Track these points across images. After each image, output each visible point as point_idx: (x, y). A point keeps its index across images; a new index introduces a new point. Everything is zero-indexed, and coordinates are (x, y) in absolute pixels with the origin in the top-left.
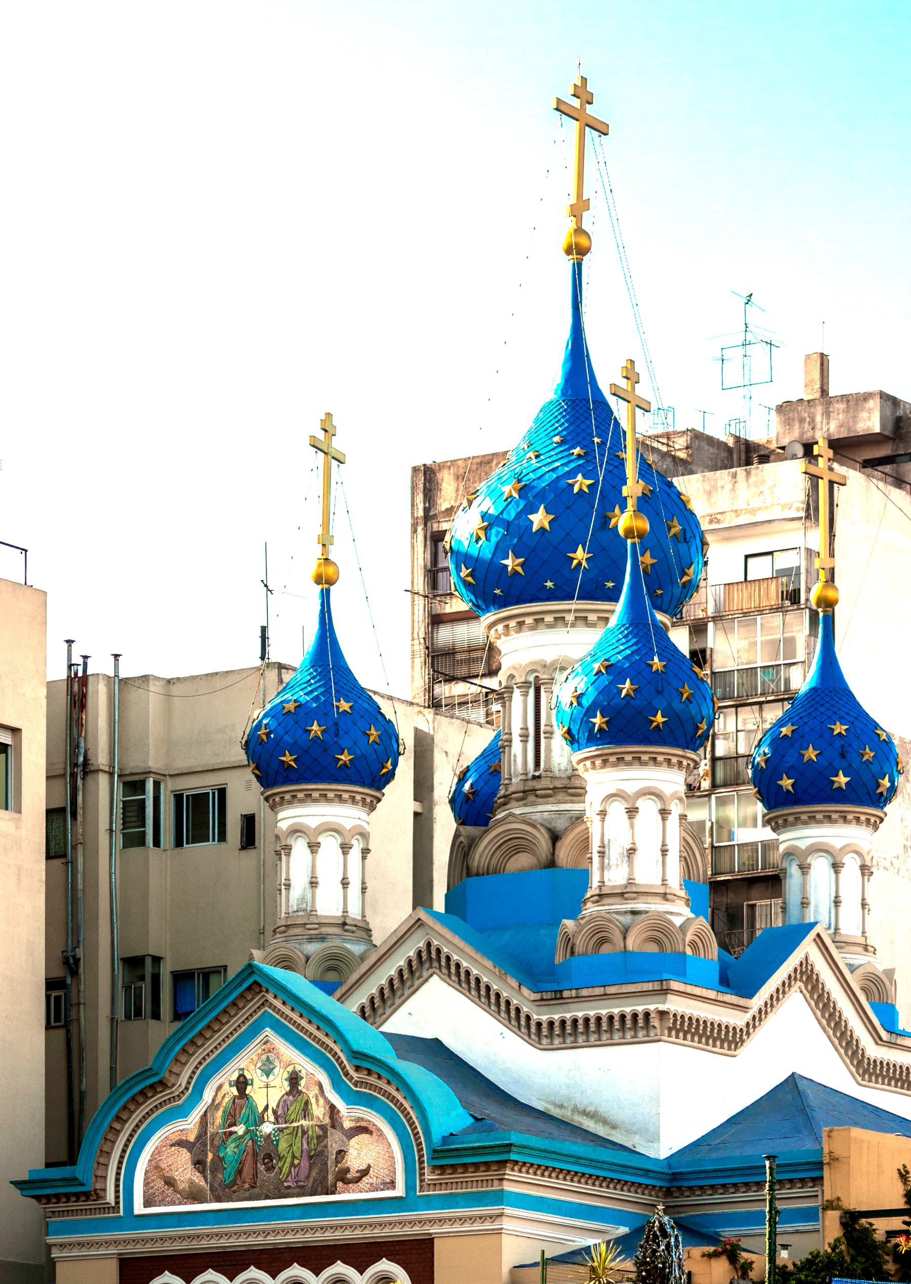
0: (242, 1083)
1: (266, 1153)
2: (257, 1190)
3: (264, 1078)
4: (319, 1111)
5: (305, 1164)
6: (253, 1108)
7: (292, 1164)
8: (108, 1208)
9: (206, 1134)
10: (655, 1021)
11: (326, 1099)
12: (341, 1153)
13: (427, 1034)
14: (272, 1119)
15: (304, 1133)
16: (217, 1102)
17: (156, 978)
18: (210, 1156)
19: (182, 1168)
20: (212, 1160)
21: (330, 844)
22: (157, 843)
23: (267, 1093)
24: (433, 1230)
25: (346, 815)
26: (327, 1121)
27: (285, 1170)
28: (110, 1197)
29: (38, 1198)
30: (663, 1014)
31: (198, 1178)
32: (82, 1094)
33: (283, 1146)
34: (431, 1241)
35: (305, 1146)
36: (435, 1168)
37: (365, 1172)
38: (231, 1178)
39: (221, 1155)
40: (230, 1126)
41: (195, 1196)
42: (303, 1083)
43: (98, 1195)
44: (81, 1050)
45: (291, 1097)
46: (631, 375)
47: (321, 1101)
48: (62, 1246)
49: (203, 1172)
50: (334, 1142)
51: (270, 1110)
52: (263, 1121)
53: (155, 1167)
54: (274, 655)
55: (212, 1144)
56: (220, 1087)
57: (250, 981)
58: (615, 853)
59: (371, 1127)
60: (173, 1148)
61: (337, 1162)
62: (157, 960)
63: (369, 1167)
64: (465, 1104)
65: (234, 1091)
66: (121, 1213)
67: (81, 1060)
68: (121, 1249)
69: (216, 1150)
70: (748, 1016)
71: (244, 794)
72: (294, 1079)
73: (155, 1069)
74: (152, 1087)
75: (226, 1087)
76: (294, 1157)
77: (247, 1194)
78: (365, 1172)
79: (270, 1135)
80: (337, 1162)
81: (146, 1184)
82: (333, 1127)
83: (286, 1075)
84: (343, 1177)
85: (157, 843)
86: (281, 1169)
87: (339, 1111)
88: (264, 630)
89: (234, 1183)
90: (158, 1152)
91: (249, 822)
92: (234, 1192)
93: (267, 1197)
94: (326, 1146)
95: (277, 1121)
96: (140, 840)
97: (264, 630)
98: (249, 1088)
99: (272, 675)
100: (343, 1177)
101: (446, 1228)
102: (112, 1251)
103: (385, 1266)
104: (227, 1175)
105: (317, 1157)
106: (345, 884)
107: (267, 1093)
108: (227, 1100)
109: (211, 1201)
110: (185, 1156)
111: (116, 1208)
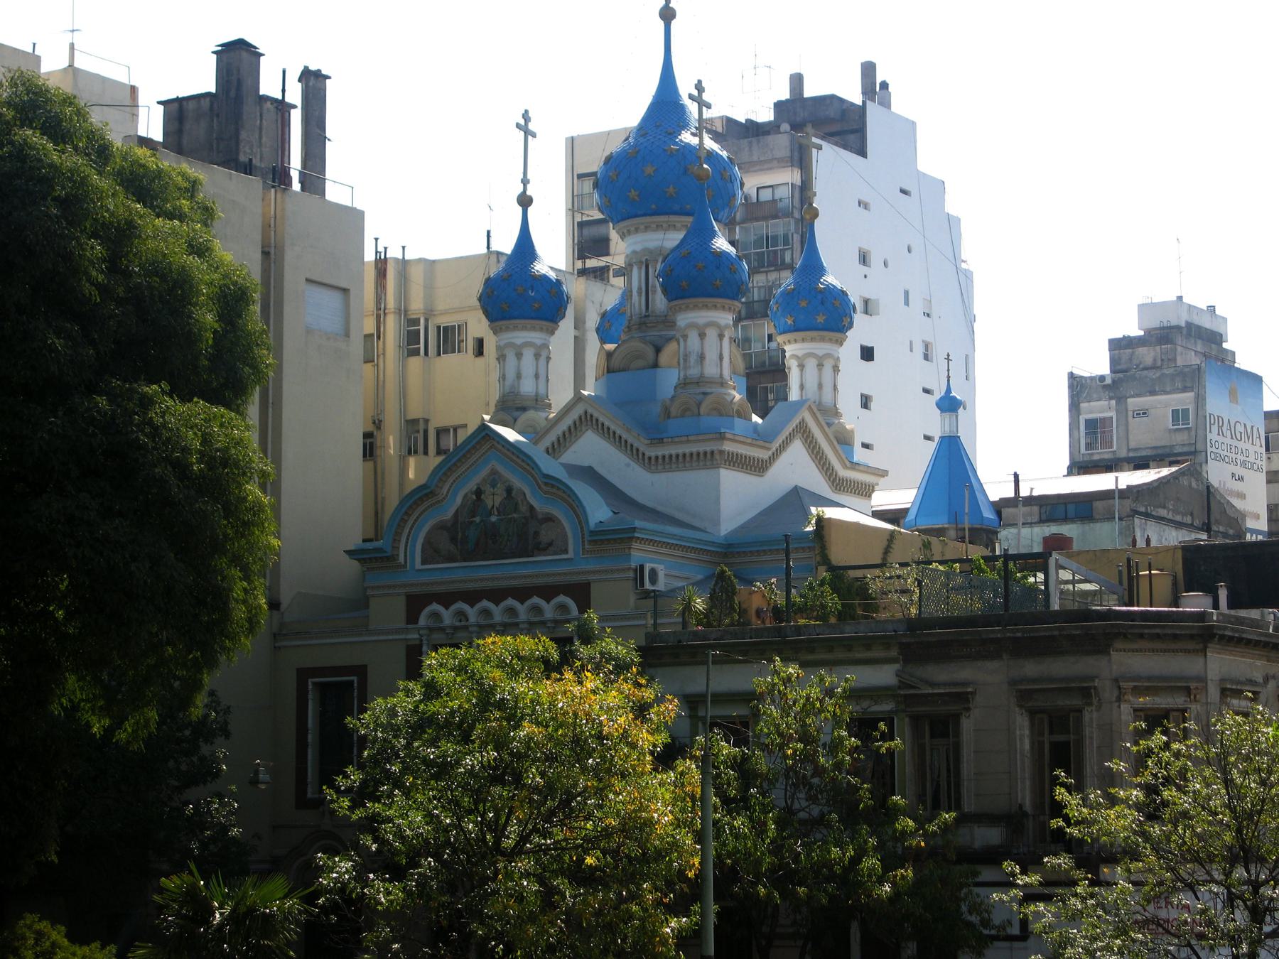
8: (400, 566)
10: (717, 456)
12: (536, 533)
13: (586, 464)
17: (426, 432)
21: (528, 355)
22: (426, 353)
23: (493, 499)
25: (536, 337)
26: (528, 514)
29: (359, 560)
30: (721, 452)
32: (383, 498)
36: (590, 542)
37: (550, 544)
41: (451, 559)
43: (393, 558)
44: (383, 473)
46: (699, 87)
48: (373, 588)
52: (490, 514)
53: (428, 543)
54: (494, 247)
56: (466, 496)
58: (693, 359)
62: (427, 421)
64: (608, 505)
67: (383, 479)
70: (770, 453)
71: (478, 326)
74: (426, 495)
78: (550, 544)
81: (423, 551)
85: (426, 353)
88: (488, 232)
90: (429, 532)
91: (480, 343)
96: (415, 353)
97: (488, 232)
99: (494, 258)
103: (562, 598)
106: (537, 376)
107: (493, 499)
111: (405, 566)
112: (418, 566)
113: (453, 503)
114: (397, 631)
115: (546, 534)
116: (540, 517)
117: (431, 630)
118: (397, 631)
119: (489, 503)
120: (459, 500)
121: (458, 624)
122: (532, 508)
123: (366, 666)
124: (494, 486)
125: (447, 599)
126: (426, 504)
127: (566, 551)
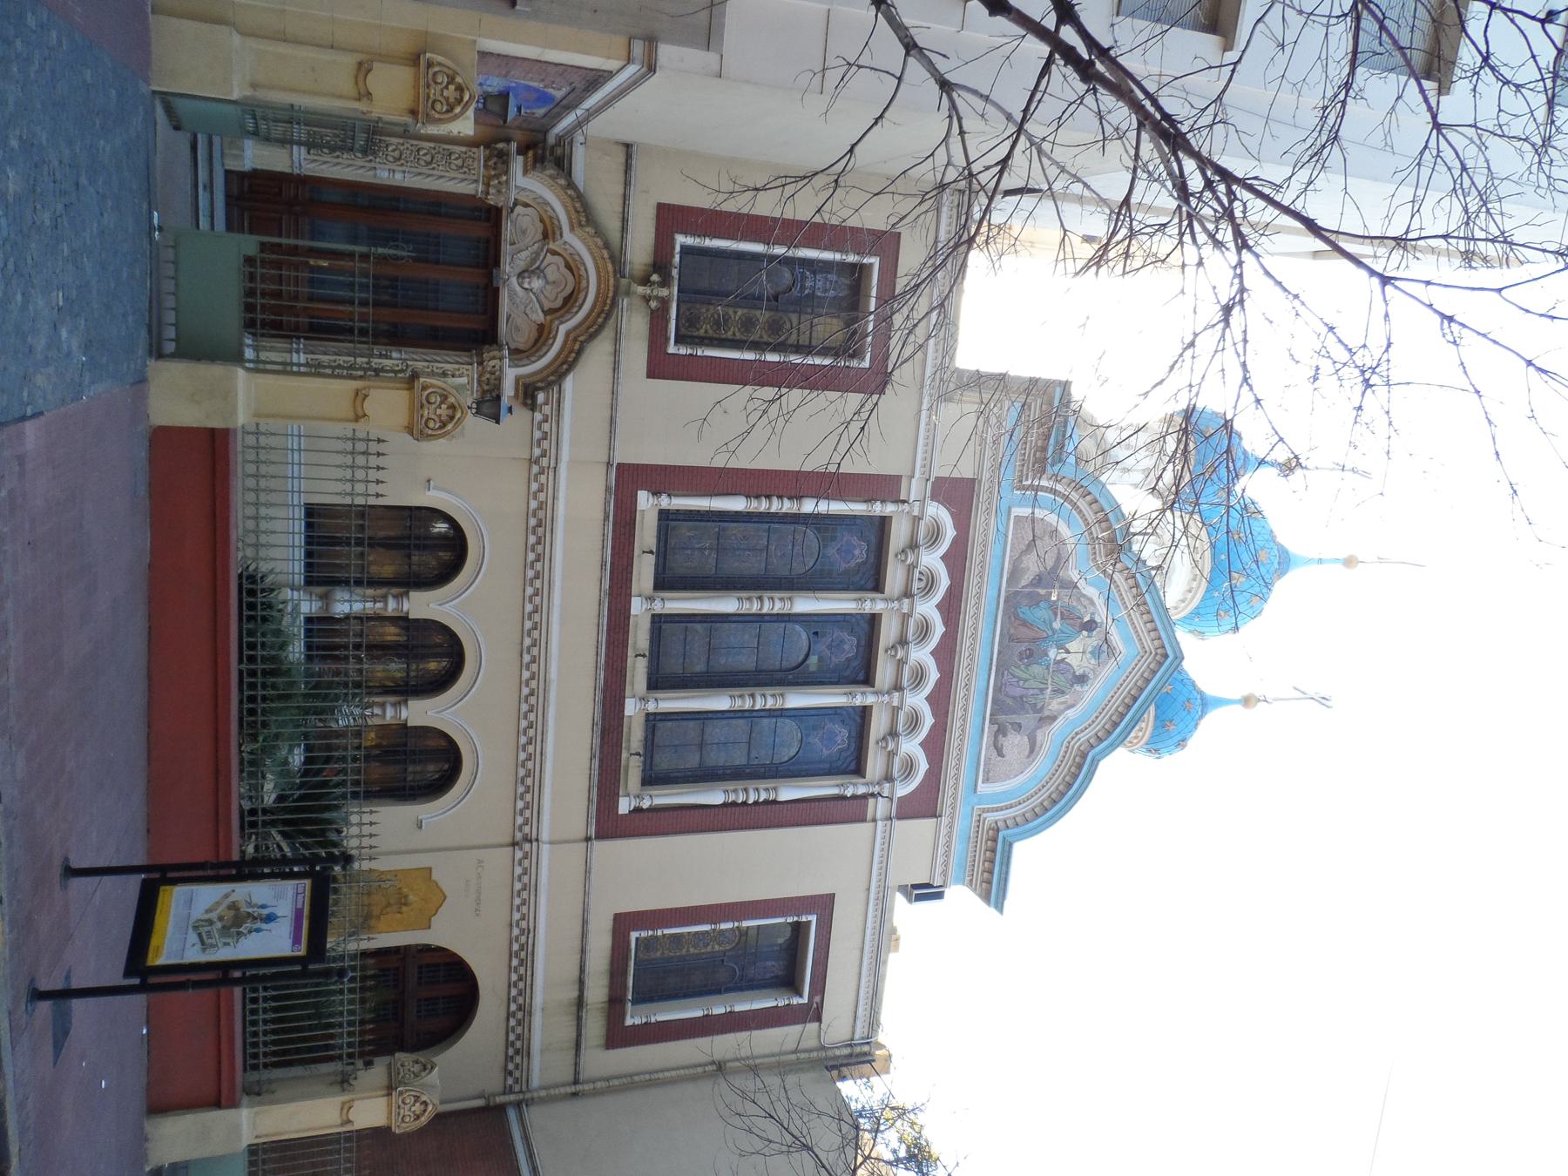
0: (1090, 626)
1: (1032, 655)
4: (1054, 705)
5: (1018, 692)
6: (1070, 638)
12: (1018, 727)
15: (1042, 690)
23: (1077, 653)
24: (945, 820)
26: (1046, 713)
27: (1020, 674)
33: (1036, 669)
34: (934, 815)
37: (1000, 754)
39: (1042, 604)
41: (1015, 574)
49: (1031, 584)
50: (1028, 719)
56: (1092, 603)
57: (1170, 652)
68: (985, 486)
72: (1082, 679)
75: (1091, 609)
78: (1000, 754)
84: (1001, 731)
86: (1018, 667)
89: (1017, 617)
93: (1000, 652)
95: (1058, 662)
98: (1085, 633)
100: (1001, 731)
101: (944, 831)
102: (986, 476)
104: (1025, 612)
105: (1021, 704)
107: (1077, 653)
113: (1089, 583)
114: (928, 464)
115: (1015, 743)
117: (916, 520)
118: (928, 464)
121: (917, 575)
122: (1054, 718)
125: (957, 559)
127: (986, 780)
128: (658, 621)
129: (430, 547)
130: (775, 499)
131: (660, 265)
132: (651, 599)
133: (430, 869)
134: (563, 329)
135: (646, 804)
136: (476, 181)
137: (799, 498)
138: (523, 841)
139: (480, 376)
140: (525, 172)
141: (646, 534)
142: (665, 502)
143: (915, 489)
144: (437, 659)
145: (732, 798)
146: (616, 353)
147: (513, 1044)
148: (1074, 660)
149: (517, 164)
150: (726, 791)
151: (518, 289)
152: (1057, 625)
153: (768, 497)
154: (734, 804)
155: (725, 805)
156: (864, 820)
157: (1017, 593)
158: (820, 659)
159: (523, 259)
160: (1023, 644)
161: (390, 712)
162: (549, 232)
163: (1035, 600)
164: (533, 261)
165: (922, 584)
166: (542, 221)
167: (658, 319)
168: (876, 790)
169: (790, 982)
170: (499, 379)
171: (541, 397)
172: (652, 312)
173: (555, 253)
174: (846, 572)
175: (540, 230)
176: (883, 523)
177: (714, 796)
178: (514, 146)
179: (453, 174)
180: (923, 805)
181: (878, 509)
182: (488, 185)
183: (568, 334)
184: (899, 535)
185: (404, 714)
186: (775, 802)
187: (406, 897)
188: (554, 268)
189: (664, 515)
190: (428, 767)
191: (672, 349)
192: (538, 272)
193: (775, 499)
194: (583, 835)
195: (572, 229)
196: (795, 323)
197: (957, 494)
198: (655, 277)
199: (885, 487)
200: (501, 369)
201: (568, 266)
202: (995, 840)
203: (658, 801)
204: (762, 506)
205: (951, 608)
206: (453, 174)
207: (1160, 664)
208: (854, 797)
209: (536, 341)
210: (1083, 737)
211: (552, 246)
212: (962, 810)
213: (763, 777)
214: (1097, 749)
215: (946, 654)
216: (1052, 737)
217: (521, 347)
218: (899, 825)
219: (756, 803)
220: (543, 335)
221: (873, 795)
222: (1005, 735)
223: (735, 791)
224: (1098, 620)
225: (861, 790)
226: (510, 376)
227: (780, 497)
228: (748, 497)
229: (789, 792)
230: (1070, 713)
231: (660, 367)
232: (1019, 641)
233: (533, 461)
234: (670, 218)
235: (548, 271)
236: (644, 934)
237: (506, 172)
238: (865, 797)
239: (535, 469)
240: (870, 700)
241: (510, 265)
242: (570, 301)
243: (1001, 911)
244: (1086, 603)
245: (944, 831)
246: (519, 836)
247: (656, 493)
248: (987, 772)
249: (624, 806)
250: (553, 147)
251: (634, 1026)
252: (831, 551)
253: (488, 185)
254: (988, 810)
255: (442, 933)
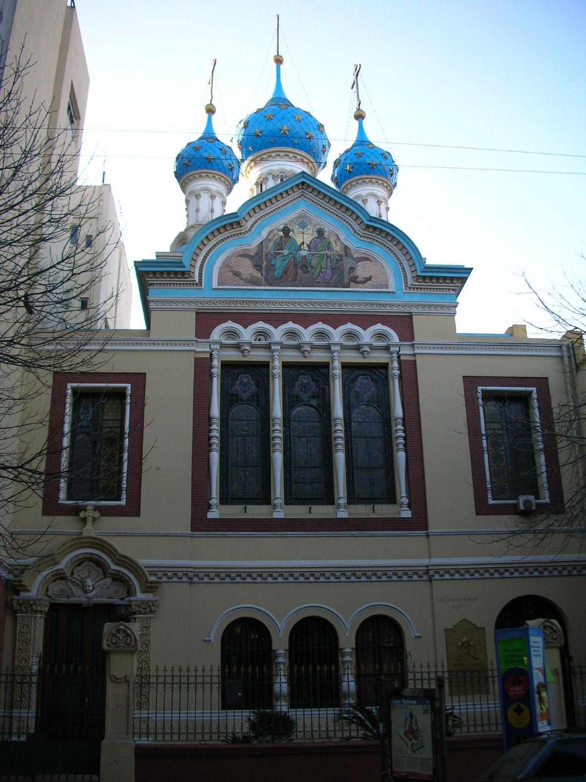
0: (286, 231)
1: (305, 265)
2: (297, 282)
3: (301, 230)
4: (337, 248)
5: (329, 271)
7: (321, 271)
8: (193, 284)
9: (262, 252)
11: (341, 242)
12: (352, 269)
14: (307, 249)
15: (328, 257)
16: (269, 238)
18: (265, 263)
19: (247, 269)
20: (266, 265)
23: (303, 237)
24: (413, 310)
26: (343, 253)
28: (197, 279)
31: (258, 274)
33: (314, 262)
34: (411, 317)
35: (329, 263)
37: (369, 279)
38: (280, 275)
40: (278, 250)
41: (254, 281)
42: (326, 234)
45: (319, 240)
47: (338, 243)
50: (347, 263)
51: (305, 245)
53: (226, 265)
55: (266, 258)
56: (271, 232)
57: (301, 181)
59: (371, 258)
60: (240, 258)
61: (350, 273)
63: (371, 277)
65: (282, 234)
66: (203, 287)
68: (199, 306)
69: (269, 261)
72: (320, 232)
73: (238, 214)
76: (322, 268)
77: (290, 284)
78: (369, 279)
79: (305, 256)
80: (350, 273)
81: (220, 274)
82: (347, 256)
83: (315, 229)
84: (355, 280)
87: (350, 249)
88: (104, 173)
89: (281, 277)
92: (281, 282)
94: (342, 265)
97: (104, 173)
98: (291, 234)
101: (420, 310)
102: (193, 306)
104: (278, 272)
105: (337, 268)
107: (303, 237)
108: (276, 237)
109: (265, 285)
110: (248, 262)
112: (215, 285)
114: (188, 342)
115: (362, 271)
116: (355, 256)
117: (223, 346)
118: (188, 342)
119: (299, 241)
120: (264, 234)
121: (257, 342)
123: (144, 375)
124: (303, 226)
125: (245, 319)
126: (226, 234)
127: (387, 286)
128: (290, 500)
129: (245, 641)
130: (211, 434)
131: (75, 511)
132: (275, 506)
133: (446, 630)
134: (113, 567)
135: (405, 500)
136: (35, 618)
137: (210, 419)
138: (428, 574)
139: (140, 613)
140: (28, 591)
141: (234, 511)
142: (215, 501)
143: (203, 348)
144: (314, 634)
145: (401, 446)
146: (126, 535)
147: (559, 572)
148: (308, 239)
149: (23, 595)
150: (398, 450)
151: (93, 593)
152: (286, 252)
153: (210, 438)
154: (405, 445)
155: (406, 451)
156: (415, 362)
157: (266, 279)
158: (313, 397)
159: (76, 591)
160: (299, 272)
161: (348, 658)
162: (60, 576)
163: (271, 268)
164: (77, 585)
165: (262, 338)
166: (55, 581)
167: (106, 512)
168: (395, 355)
169: (523, 399)
170: (142, 602)
171: (153, 578)
172: (102, 515)
173: (72, 573)
174: (257, 386)
175: (58, 582)
176: (225, 365)
177: (401, 457)
178: (16, 597)
179: (32, 631)
180: (404, 324)
181: (216, 370)
182: (36, 612)
183: (116, 564)
184: (233, 356)
185: (348, 650)
186: (404, 419)
187: (463, 643)
188: (81, 572)
189: (223, 501)
190: (382, 633)
191: (123, 502)
192: (83, 581)
193: (211, 434)
194: (425, 538)
195: (57, 564)
196: (108, 430)
197: (206, 321)
198: (82, 515)
199: (202, 367)
200: (137, 601)
201: (79, 565)
202: (424, 278)
203: (404, 494)
204: (215, 441)
205: (276, 319)
206: (32, 631)
207: (308, 186)
208: (400, 369)
209: (122, 582)
210: (357, 228)
211: (68, 575)
212: (407, 299)
213: (390, 427)
214: (363, 219)
215: (306, 319)
216: (357, 246)
217: (126, 590)
218: (417, 339)
219: (404, 431)
220: (118, 578)
221: (399, 357)
222: (357, 277)
223: (397, 445)
224: (282, 227)
225: (396, 364)
226: (140, 596)
227: (210, 431)
228: (210, 451)
229: (398, 411)
230: (342, 238)
231: (133, 509)
232: (296, 274)
233: (191, 582)
234: (51, 508)
235: (83, 576)
236: (490, 496)
237: (29, 601)
238: (400, 362)
239: (195, 579)
240: (337, 364)
241: (78, 597)
242: (98, 563)
243: (471, 269)
244: (272, 235)
245: (420, 310)
246: (425, 577)
247: (209, 507)
248: (381, 286)
249: (407, 514)
250: (15, 576)
251: (550, 498)
252: (245, 396)
253: (36, 612)
254: (406, 283)
255: (487, 619)
